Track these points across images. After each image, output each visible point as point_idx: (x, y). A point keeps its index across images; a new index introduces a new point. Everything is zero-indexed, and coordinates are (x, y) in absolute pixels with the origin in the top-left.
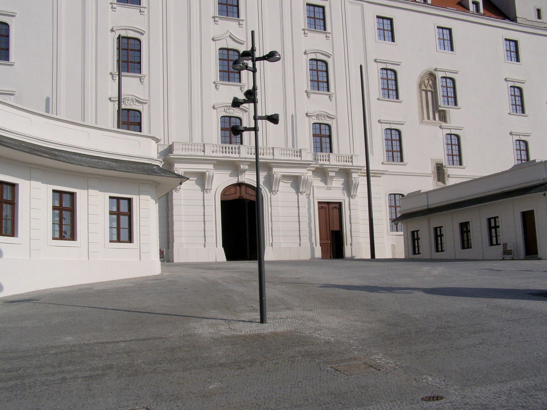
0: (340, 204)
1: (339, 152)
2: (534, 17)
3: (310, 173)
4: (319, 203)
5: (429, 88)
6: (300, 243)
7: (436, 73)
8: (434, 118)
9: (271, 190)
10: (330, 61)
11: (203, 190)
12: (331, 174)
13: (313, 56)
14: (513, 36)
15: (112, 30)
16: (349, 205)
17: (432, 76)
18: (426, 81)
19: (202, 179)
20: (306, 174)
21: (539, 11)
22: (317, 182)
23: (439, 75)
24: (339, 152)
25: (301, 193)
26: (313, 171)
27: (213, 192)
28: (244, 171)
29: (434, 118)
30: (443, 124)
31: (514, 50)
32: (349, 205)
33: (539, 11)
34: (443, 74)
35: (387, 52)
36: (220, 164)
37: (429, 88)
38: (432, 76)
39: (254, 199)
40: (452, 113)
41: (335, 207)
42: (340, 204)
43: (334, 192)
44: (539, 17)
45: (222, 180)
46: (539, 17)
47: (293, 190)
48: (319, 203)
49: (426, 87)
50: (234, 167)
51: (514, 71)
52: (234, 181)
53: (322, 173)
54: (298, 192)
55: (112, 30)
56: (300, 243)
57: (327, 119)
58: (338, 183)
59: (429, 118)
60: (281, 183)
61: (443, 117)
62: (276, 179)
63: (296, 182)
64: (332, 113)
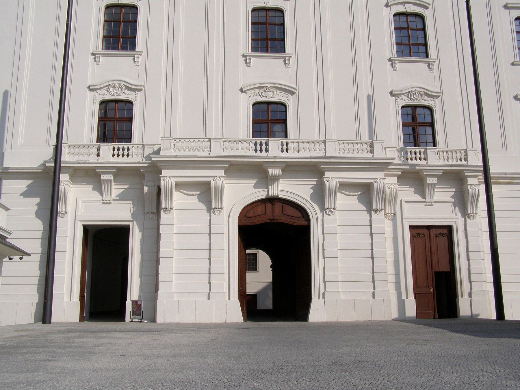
0: (449, 228)
1: (447, 145)
3: (394, 180)
4: (412, 227)
6: (374, 293)
9: (323, 209)
11: (210, 209)
12: (430, 180)
16: (466, 229)
19: (206, 192)
20: (387, 182)
22: (407, 195)
24: (447, 145)
25: (376, 211)
26: (399, 178)
27: (225, 212)
28: (275, 179)
32: (466, 229)
36: (236, 169)
39: (303, 223)
41: (441, 234)
42: (449, 228)
43: (438, 208)
45: (238, 195)
47: (363, 208)
48: (412, 227)
50: (258, 171)
52: (261, 194)
53: (414, 179)
54: (370, 210)
56: (374, 293)
57: (426, 98)
58: (444, 194)
60: (339, 194)
62: (330, 189)
63: (366, 193)
64: (434, 88)
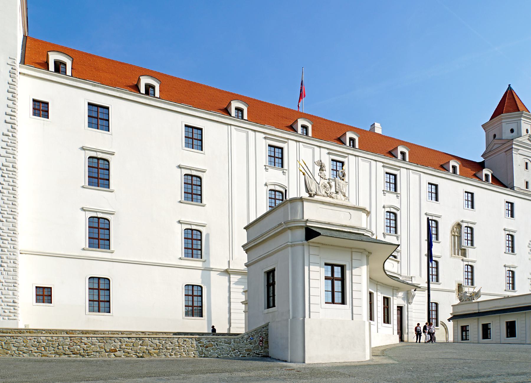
5: (456, 234)
7: (462, 223)
8: (458, 254)
10: (398, 213)
13: (388, 209)
14: (511, 199)
15: (266, 185)
17: (459, 225)
18: (455, 229)
21: (527, 183)
23: (464, 225)
29: (458, 254)
30: (464, 258)
33: (527, 183)
34: (466, 225)
35: (432, 208)
37: (456, 234)
38: (459, 225)
40: (470, 251)
49: (455, 233)
51: (510, 224)
55: (266, 185)
59: (455, 254)
61: (464, 254)
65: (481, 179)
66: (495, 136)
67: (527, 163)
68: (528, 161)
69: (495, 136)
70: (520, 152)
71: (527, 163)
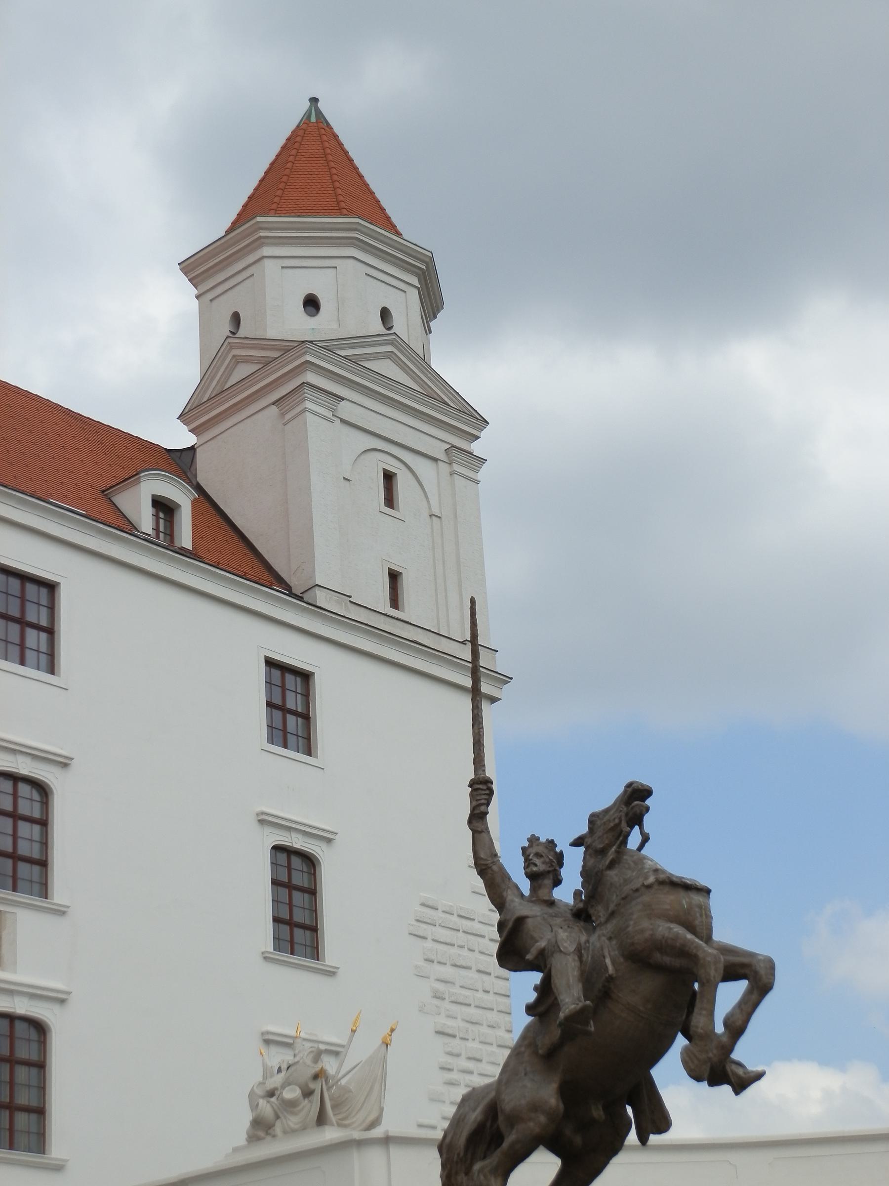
2: (379, 597)
14: (296, 652)
21: (394, 576)
31: (290, 706)
33: (394, 576)
44: (395, 602)
46: (395, 602)
65: (126, 526)
66: (236, 319)
67: (389, 477)
68: (393, 466)
69: (236, 319)
70: (345, 410)
71: (389, 477)
